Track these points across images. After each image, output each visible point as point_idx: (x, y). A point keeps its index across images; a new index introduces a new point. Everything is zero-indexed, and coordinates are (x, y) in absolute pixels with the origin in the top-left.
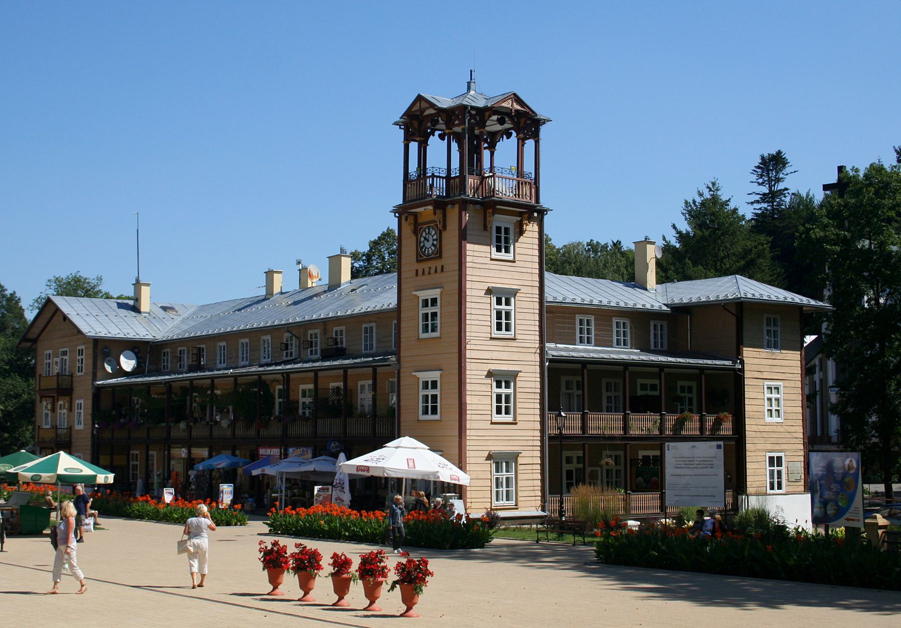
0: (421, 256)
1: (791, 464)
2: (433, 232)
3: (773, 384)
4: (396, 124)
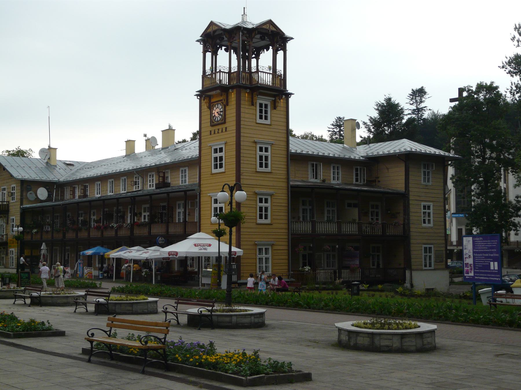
0: (213, 122)
2: (221, 107)
4: (198, 41)
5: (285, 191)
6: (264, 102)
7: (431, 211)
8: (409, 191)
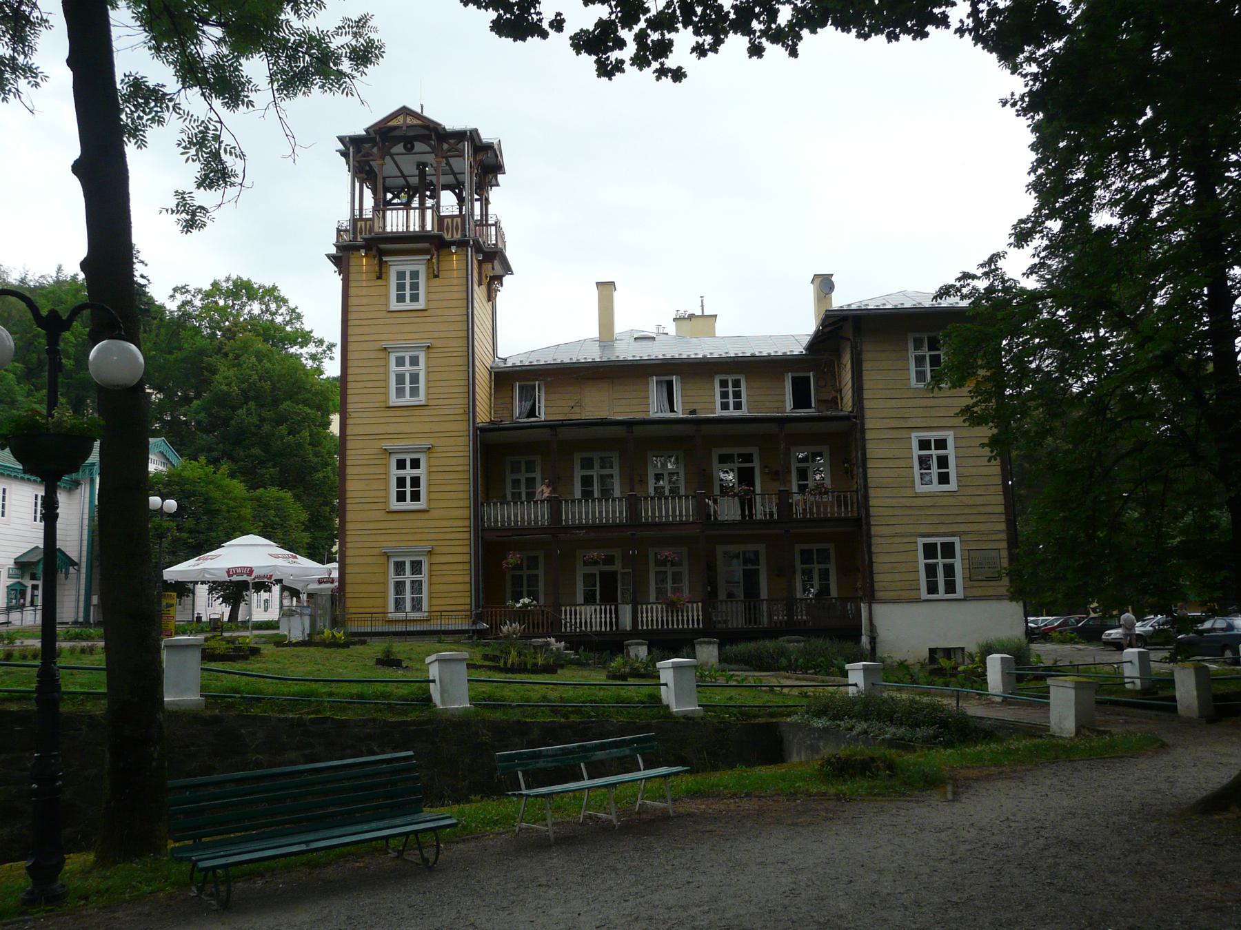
3: (932, 435)
6: (408, 269)
7: (950, 452)
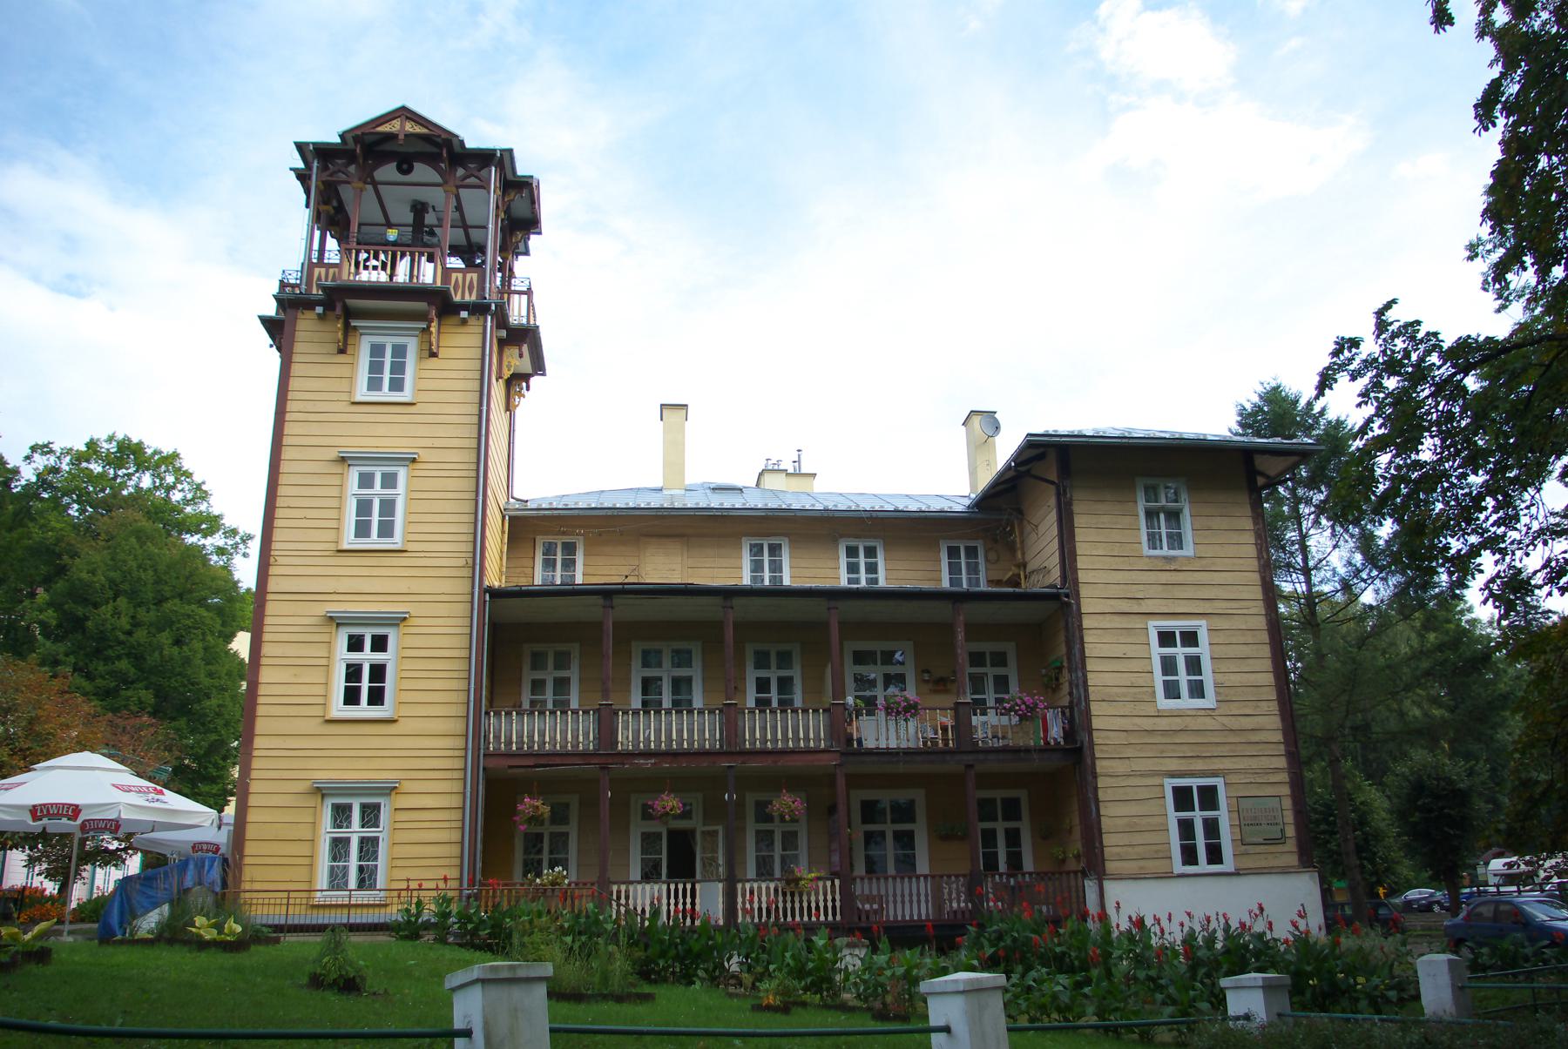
1: (1245, 804)
5: (463, 609)
7: (1203, 650)
8: (1076, 582)
